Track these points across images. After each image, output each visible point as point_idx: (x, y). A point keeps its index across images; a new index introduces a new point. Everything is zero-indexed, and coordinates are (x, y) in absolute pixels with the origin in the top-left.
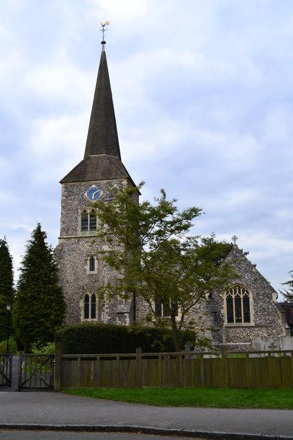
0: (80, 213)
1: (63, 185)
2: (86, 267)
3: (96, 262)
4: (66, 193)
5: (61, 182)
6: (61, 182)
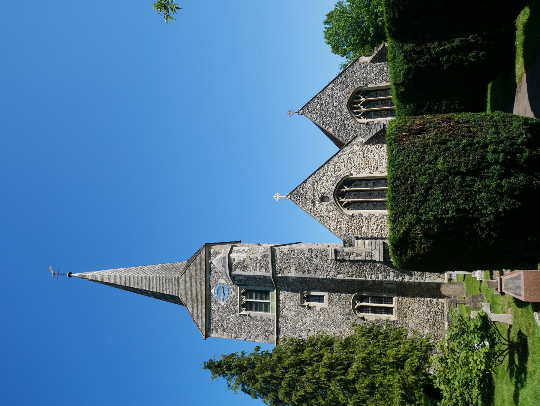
2: (318, 309)
3: (312, 293)
4: (219, 330)
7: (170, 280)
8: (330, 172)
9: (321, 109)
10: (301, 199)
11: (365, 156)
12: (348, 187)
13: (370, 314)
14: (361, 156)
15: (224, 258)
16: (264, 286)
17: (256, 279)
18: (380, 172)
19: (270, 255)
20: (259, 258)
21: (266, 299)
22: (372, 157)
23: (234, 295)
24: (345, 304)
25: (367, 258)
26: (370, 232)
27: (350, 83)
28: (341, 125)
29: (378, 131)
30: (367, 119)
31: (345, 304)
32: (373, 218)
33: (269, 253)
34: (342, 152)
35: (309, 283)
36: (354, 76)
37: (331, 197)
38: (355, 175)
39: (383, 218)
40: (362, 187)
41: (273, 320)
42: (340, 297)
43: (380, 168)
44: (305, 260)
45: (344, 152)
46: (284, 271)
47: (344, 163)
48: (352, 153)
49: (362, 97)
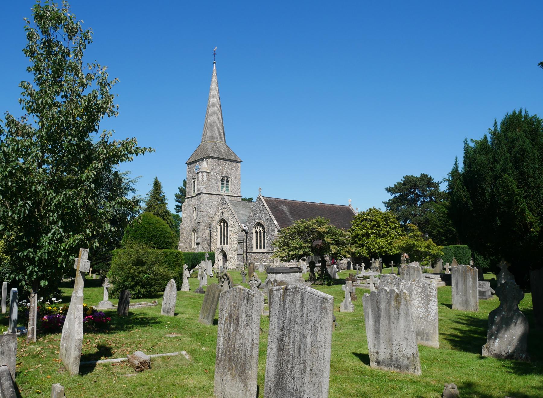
37: (222, 218)
38: (229, 228)
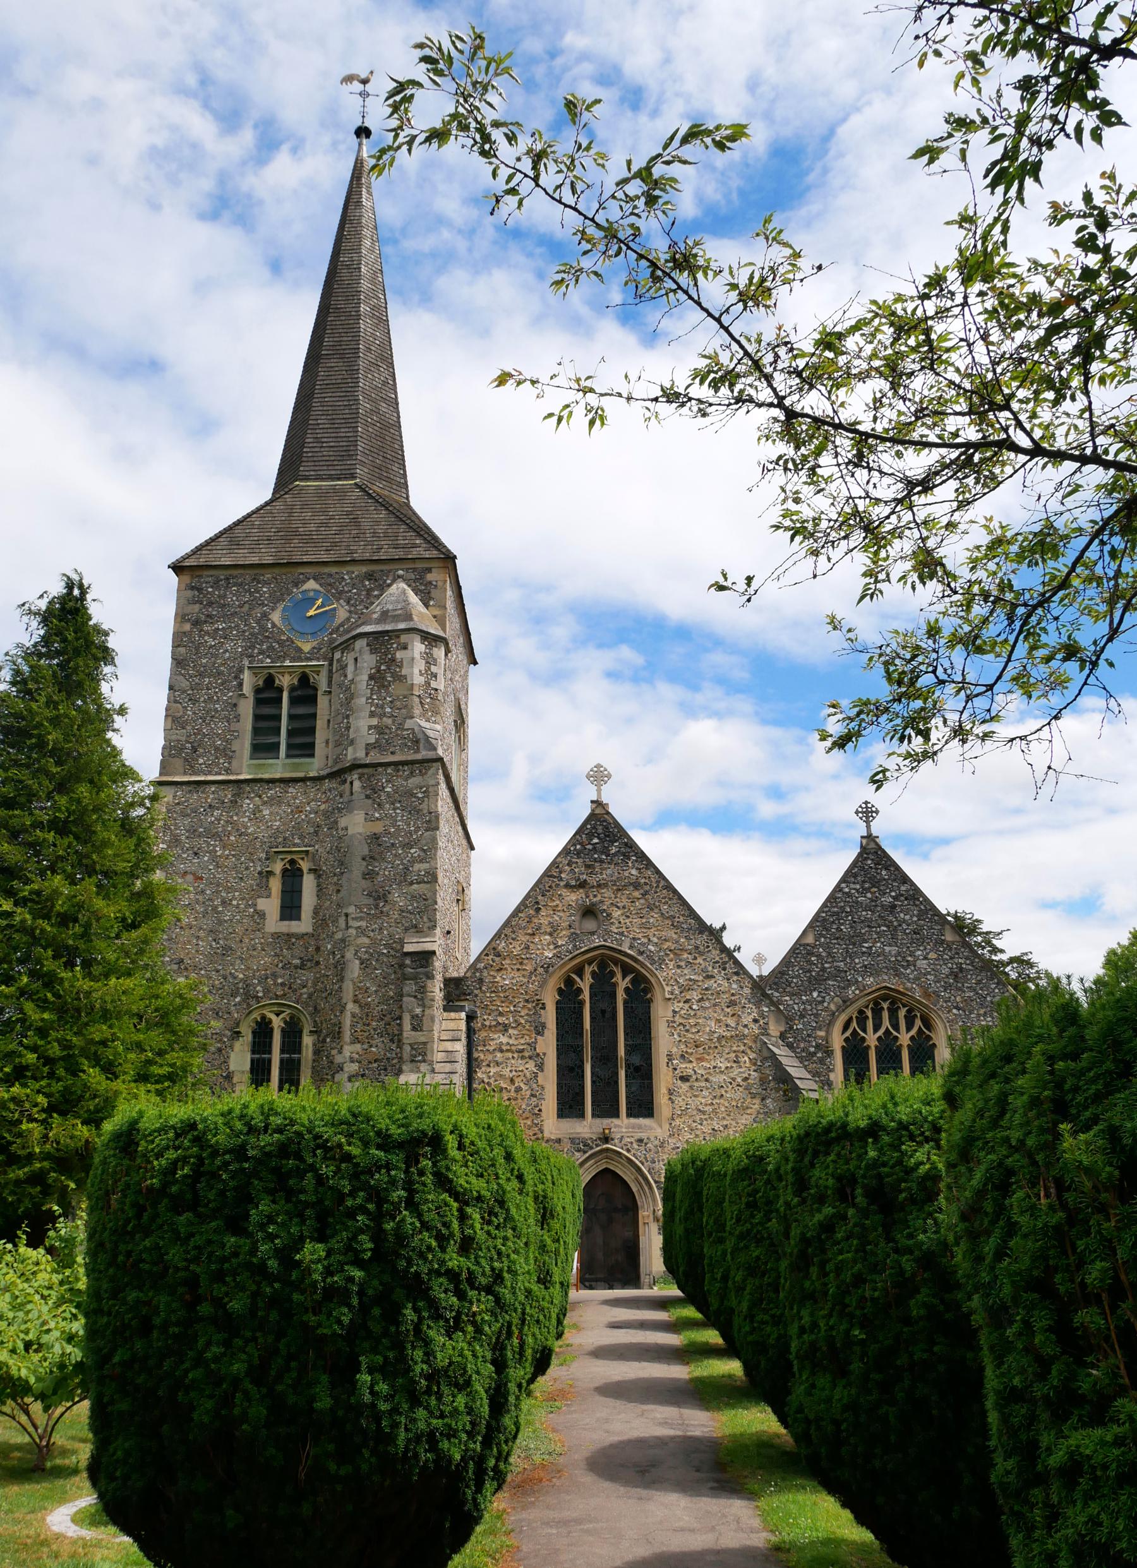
0: (247, 689)
1: (187, 579)
2: (262, 904)
4: (197, 607)
5: (177, 568)
6: (177, 568)
7: (348, 452)
8: (675, 936)
9: (876, 906)
10: (590, 847)
11: (723, 1043)
12: (627, 990)
13: (248, 1057)
14: (721, 1031)
15: (408, 617)
16: (327, 742)
17: (348, 717)
18: (671, 1087)
19: (419, 757)
20: (409, 724)
21: (289, 746)
22: (720, 1065)
23: (299, 650)
24: (275, 984)
25: (407, 1048)
26: (490, 1057)
27: (958, 999)
28: (823, 969)
29: (798, 1082)
30: (843, 1047)
31: (275, 984)
32: (531, 1065)
33: (424, 754)
34: (737, 974)
35: (335, 875)
36: (982, 1011)
39: (532, 1095)
40: (626, 1034)
41: (228, 771)
42: (296, 967)
43: (685, 1086)
44: (403, 864)
45: (735, 978)
46: (370, 801)
47: (701, 978)
48: (732, 1004)
49: (913, 1032)
